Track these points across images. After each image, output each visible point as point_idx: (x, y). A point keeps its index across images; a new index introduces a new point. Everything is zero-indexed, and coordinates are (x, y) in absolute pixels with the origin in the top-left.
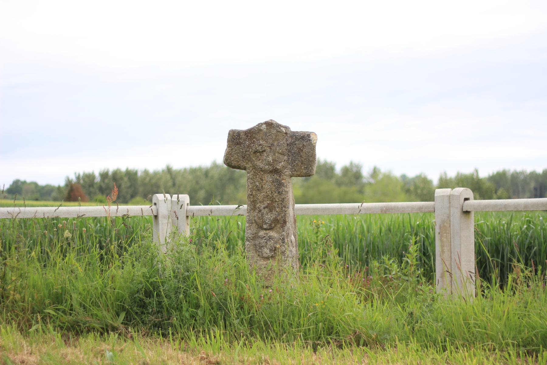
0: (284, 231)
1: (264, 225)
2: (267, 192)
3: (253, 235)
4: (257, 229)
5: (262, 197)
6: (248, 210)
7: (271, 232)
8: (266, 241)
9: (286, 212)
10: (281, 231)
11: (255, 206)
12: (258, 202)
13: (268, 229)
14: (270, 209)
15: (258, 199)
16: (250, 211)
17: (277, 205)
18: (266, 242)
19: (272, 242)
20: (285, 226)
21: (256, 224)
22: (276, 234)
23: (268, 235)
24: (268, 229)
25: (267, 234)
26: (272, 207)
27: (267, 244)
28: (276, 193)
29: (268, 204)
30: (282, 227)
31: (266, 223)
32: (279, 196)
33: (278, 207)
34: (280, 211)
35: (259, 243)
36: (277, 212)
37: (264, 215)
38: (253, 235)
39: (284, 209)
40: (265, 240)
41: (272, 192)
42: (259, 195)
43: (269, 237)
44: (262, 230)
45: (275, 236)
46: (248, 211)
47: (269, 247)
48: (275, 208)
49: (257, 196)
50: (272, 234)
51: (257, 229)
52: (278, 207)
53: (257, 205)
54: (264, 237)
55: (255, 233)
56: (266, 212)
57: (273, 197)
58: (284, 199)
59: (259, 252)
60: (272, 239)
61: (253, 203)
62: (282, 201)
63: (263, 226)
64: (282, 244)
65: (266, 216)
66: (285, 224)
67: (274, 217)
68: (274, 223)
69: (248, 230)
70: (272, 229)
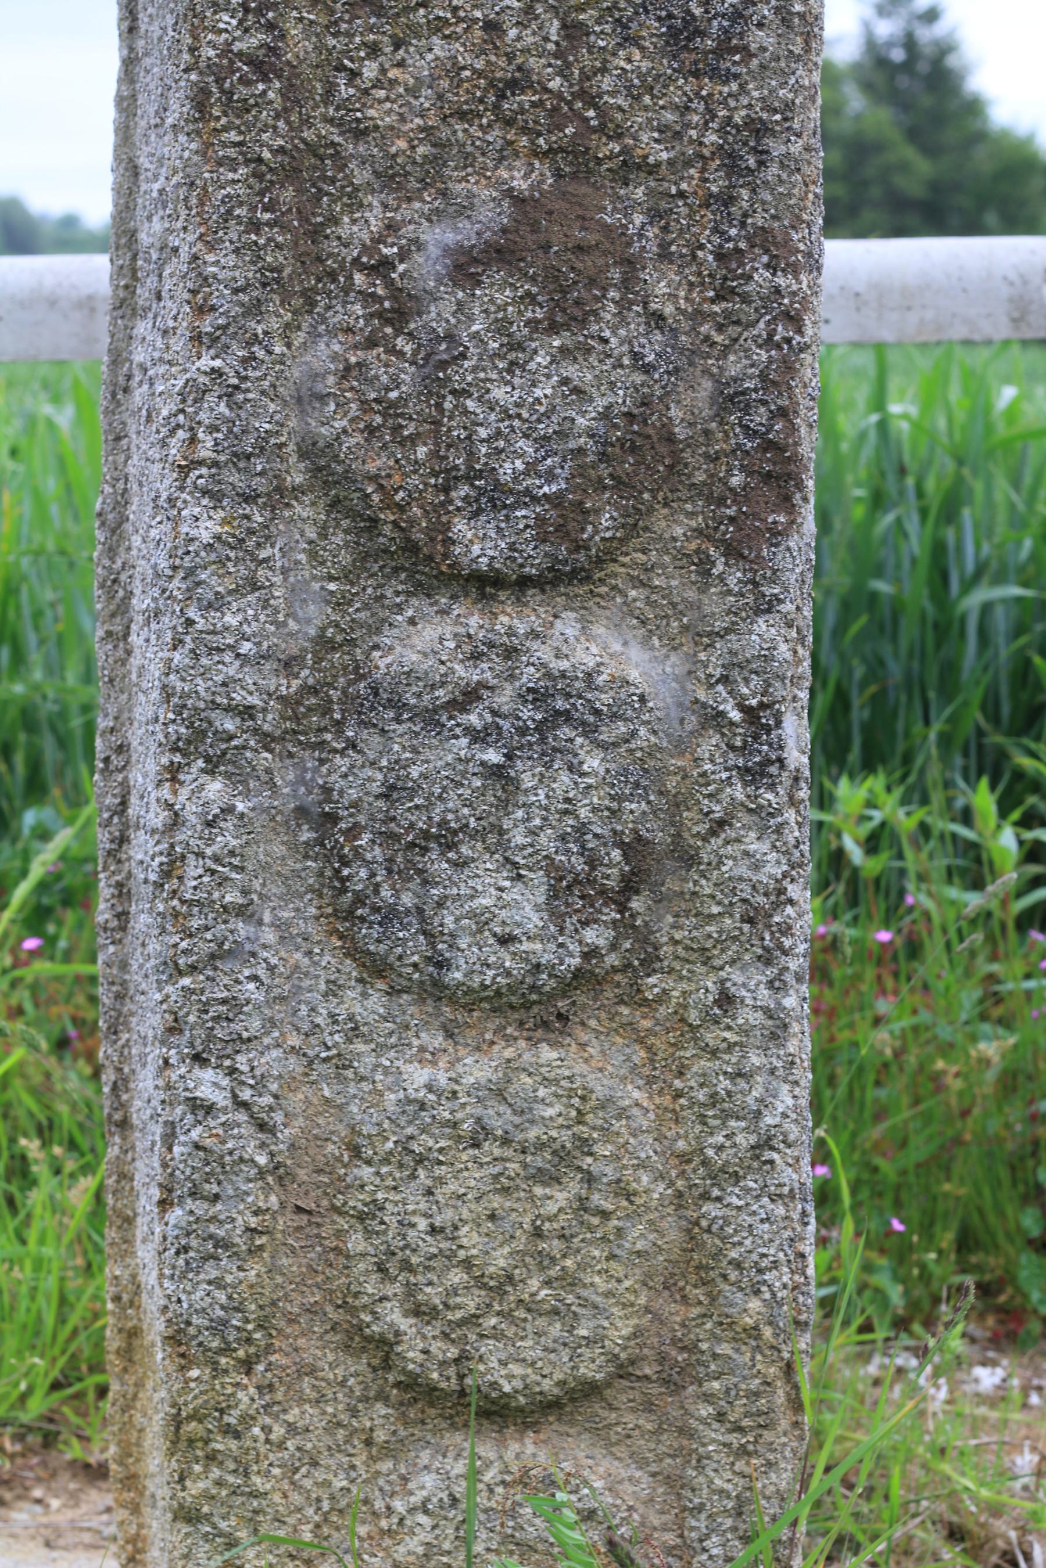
0: (767, 607)
1: (461, 527)
2: (492, 27)
3: (289, 665)
4: (347, 576)
5: (425, 99)
6: (221, 297)
7: (568, 626)
8: (493, 756)
9: (795, 320)
10: (714, 604)
11: (316, 233)
12: (361, 176)
13: (524, 583)
14: (553, 275)
15: (359, 134)
16: (255, 309)
17: (655, 215)
18: (495, 772)
19: (593, 762)
20: (776, 535)
21: (334, 504)
22: (635, 653)
23: (529, 675)
24: (524, 583)
25: (510, 653)
26: (580, 249)
27: (504, 805)
28: (630, 40)
29: (518, 200)
30: (732, 552)
31: (498, 486)
32: (681, 88)
33: (664, 255)
34: (698, 316)
35: (389, 793)
36: (657, 319)
37: (462, 375)
38: (289, 665)
39: (761, 276)
40: (479, 737)
41: (574, 32)
42: (370, 70)
43: (536, 696)
44: (423, 589)
45: (634, 675)
46: (202, 310)
47: (546, 841)
48: (631, 264)
49: (345, 91)
50: (586, 657)
51: (347, 576)
52: (664, 255)
53: (346, 228)
54: (471, 695)
55: (324, 644)
56: (501, 327)
57: (591, 100)
58: (758, 129)
59: (390, 916)
60: (589, 731)
61: (288, 194)
62: (732, 165)
63: (441, 531)
64: (739, 792)
65: (499, 393)
66: (787, 503)
67: (621, 399)
68: (620, 484)
69: (216, 604)
70: (579, 575)
